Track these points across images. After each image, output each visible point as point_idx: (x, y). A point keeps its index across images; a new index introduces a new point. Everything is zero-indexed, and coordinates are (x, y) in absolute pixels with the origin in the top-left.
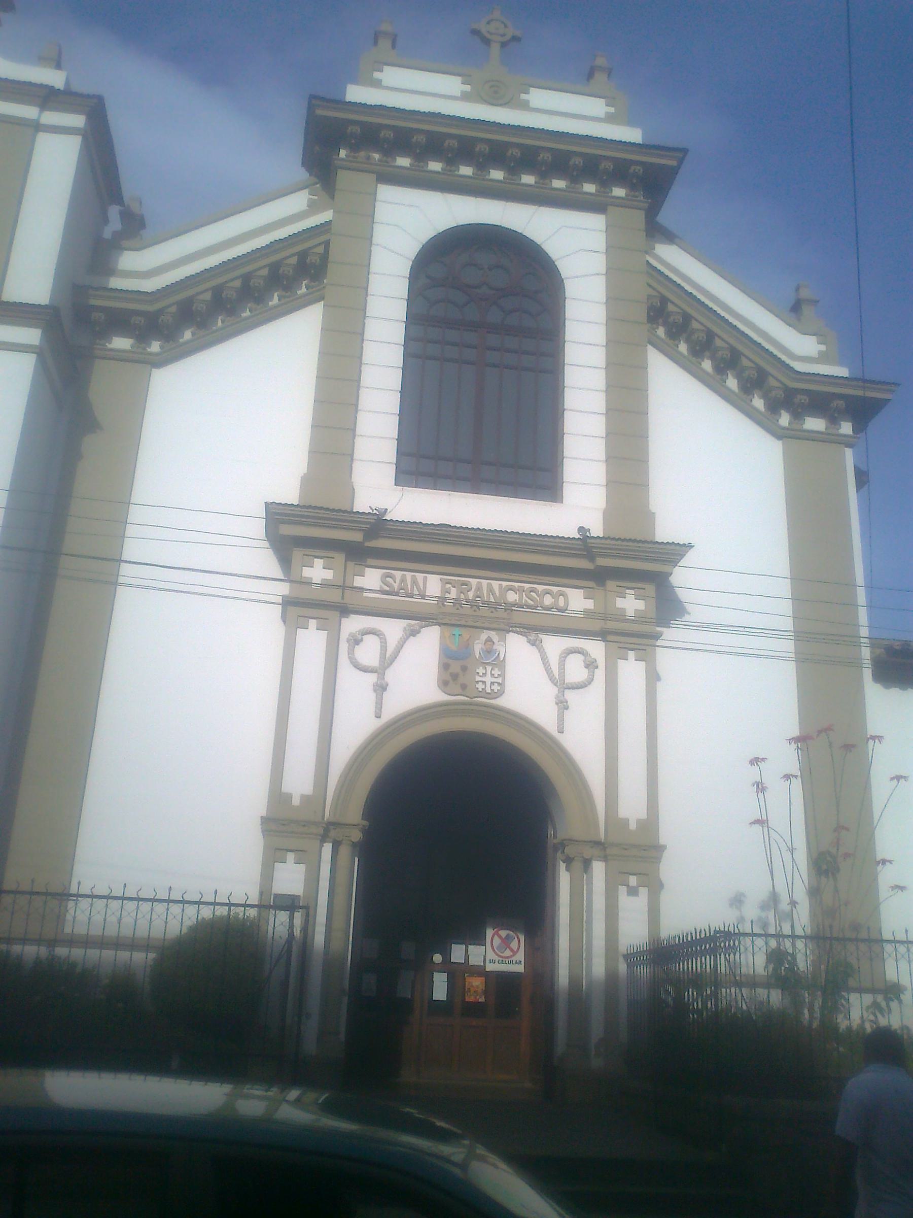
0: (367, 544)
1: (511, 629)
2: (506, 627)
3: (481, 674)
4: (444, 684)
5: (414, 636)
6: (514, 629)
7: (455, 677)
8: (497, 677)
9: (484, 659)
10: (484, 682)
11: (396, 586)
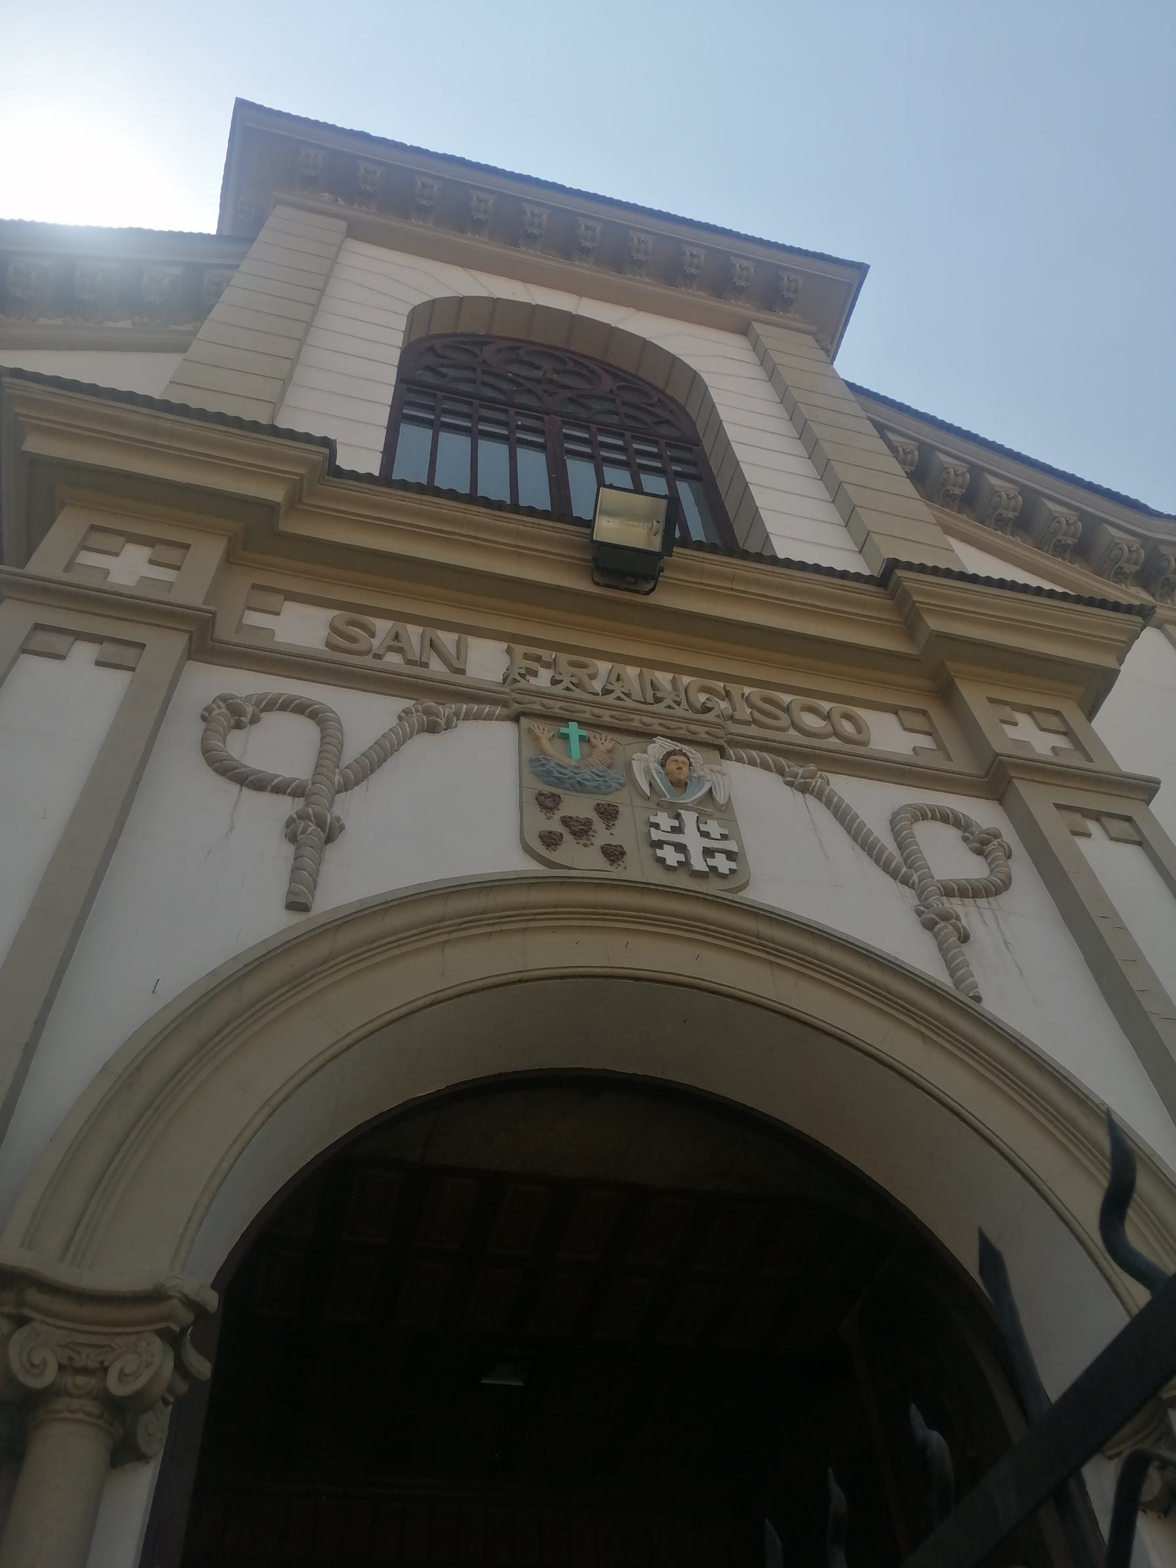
2: (722, 742)
6: (743, 753)
9: (668, 797)
10: (681, 848)
11: (375, 642)
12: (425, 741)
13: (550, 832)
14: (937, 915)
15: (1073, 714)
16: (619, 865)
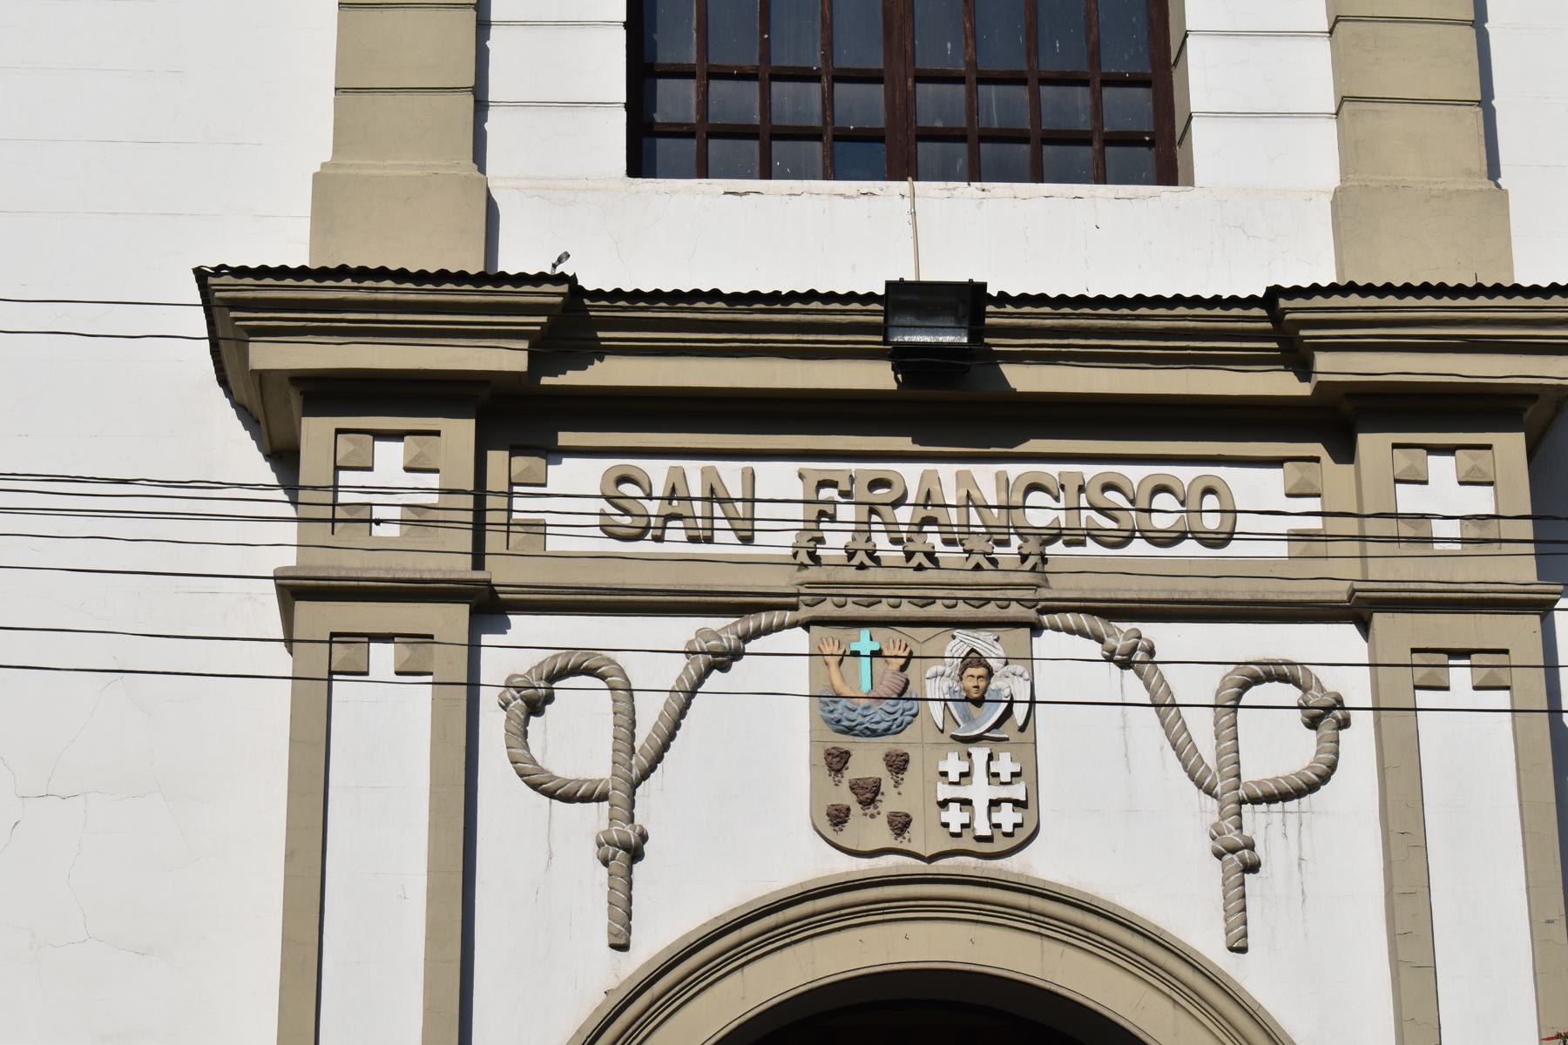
0: (546, 381)
1: (1045, 618)
2: (1031, 614)
3: (954, 777)
4: (839, 817)
5: (724, 668)
6: (1057, 618)
7: (869, 794)
8: (1010, 783)
9: (962, 725)
10: (966, 803)
12: (716, 679)
13: (837, 810)
14: (1225, 849)
15: (1510, 447)
16: (904, 838)
